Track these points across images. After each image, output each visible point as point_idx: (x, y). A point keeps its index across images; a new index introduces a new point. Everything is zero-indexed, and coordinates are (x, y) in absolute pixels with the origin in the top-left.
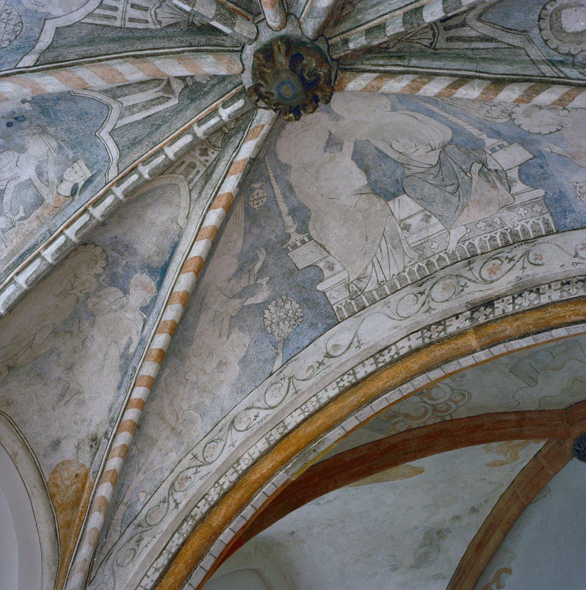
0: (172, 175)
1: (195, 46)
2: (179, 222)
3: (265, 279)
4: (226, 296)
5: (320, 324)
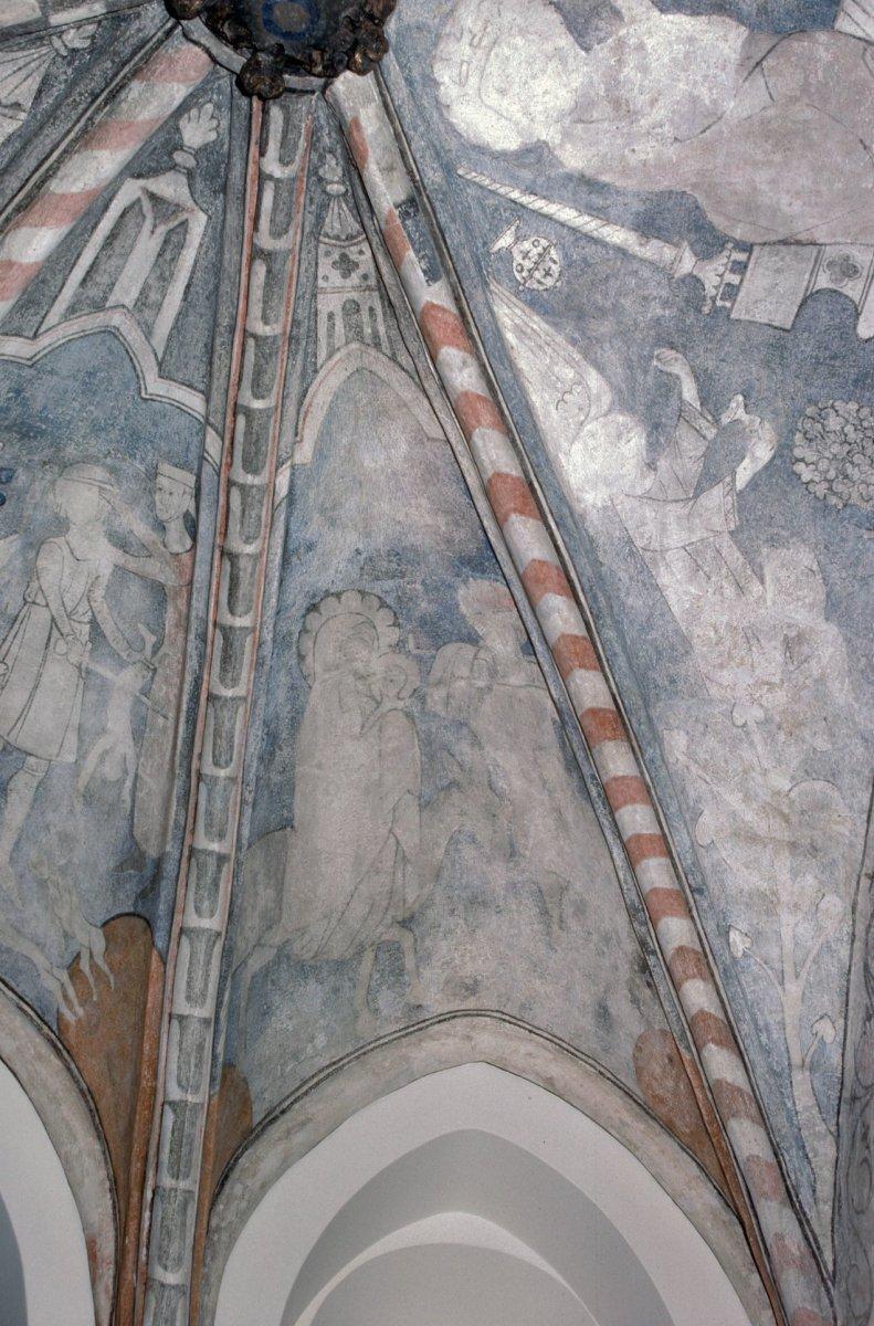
1: (102, 91)
3: (733, 405)
4: (677, 501)
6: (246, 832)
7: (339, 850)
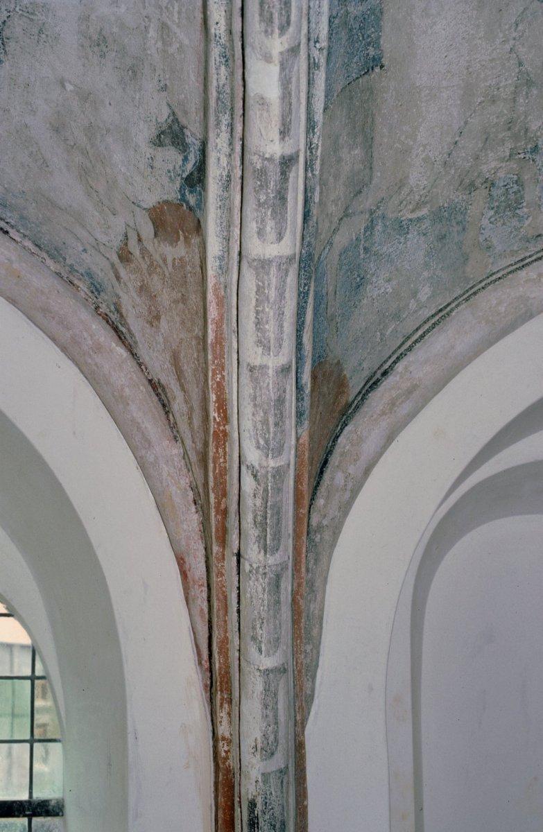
6: (319, 105)
7: (444, 83)
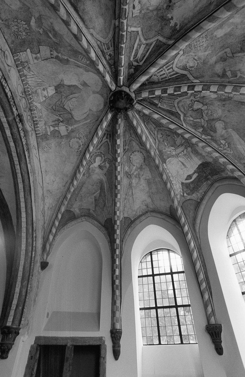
0: (110, 40)
2: (92, 29)
5: (13, 45)
